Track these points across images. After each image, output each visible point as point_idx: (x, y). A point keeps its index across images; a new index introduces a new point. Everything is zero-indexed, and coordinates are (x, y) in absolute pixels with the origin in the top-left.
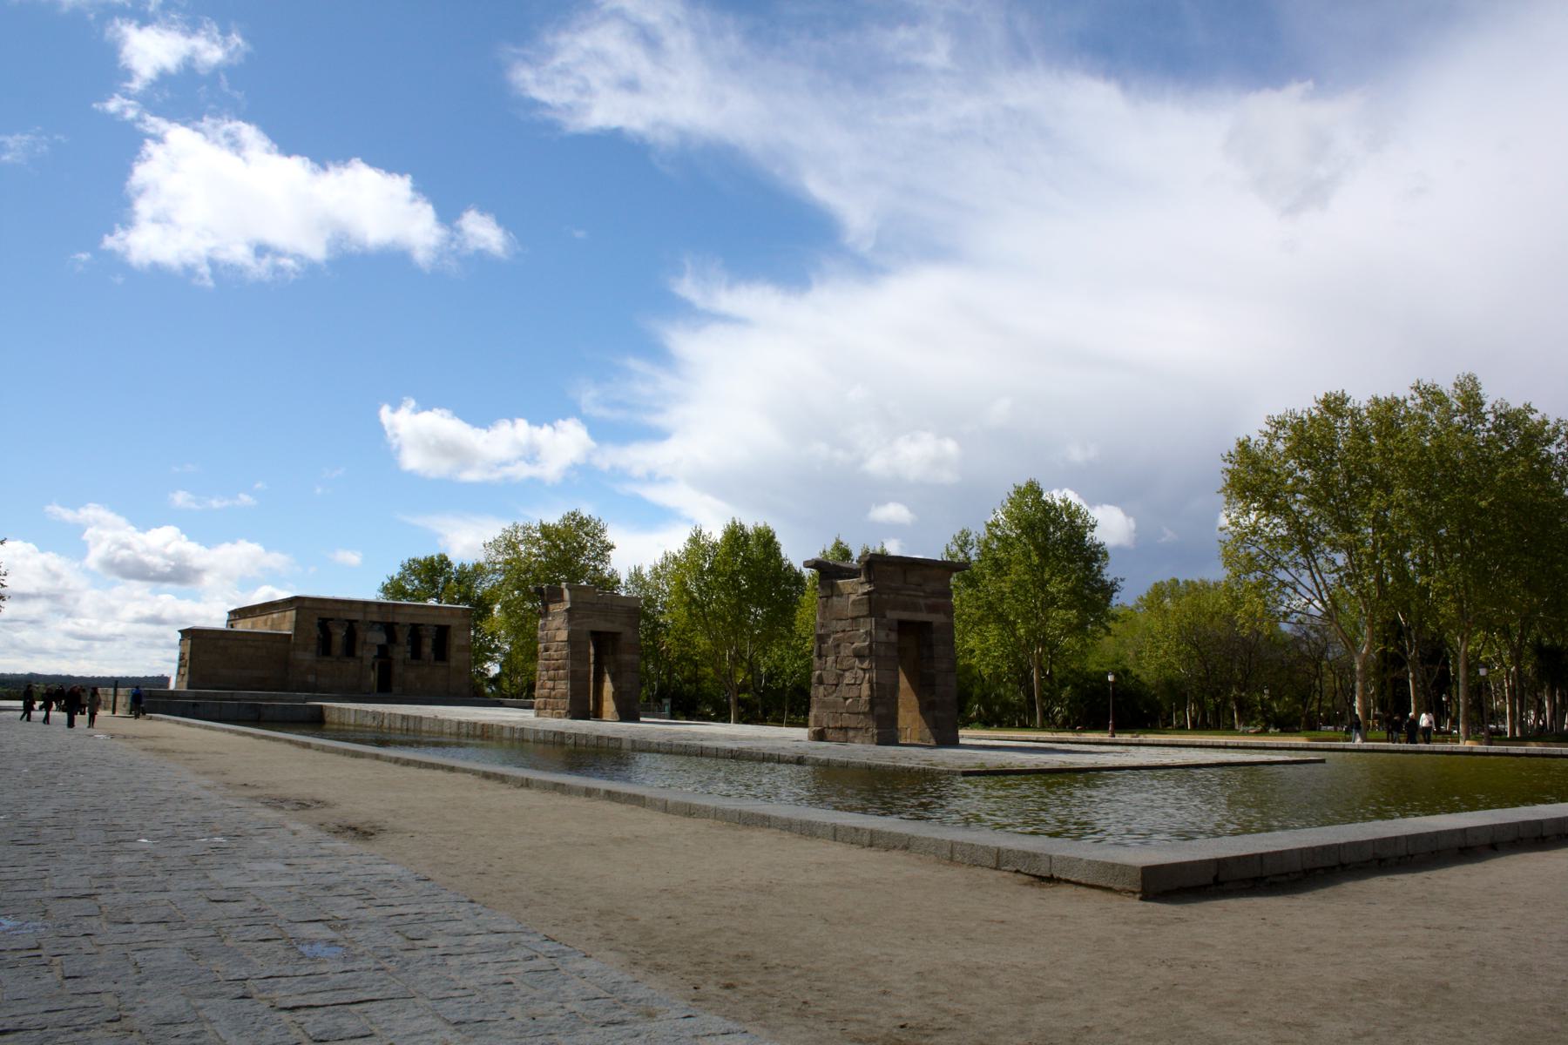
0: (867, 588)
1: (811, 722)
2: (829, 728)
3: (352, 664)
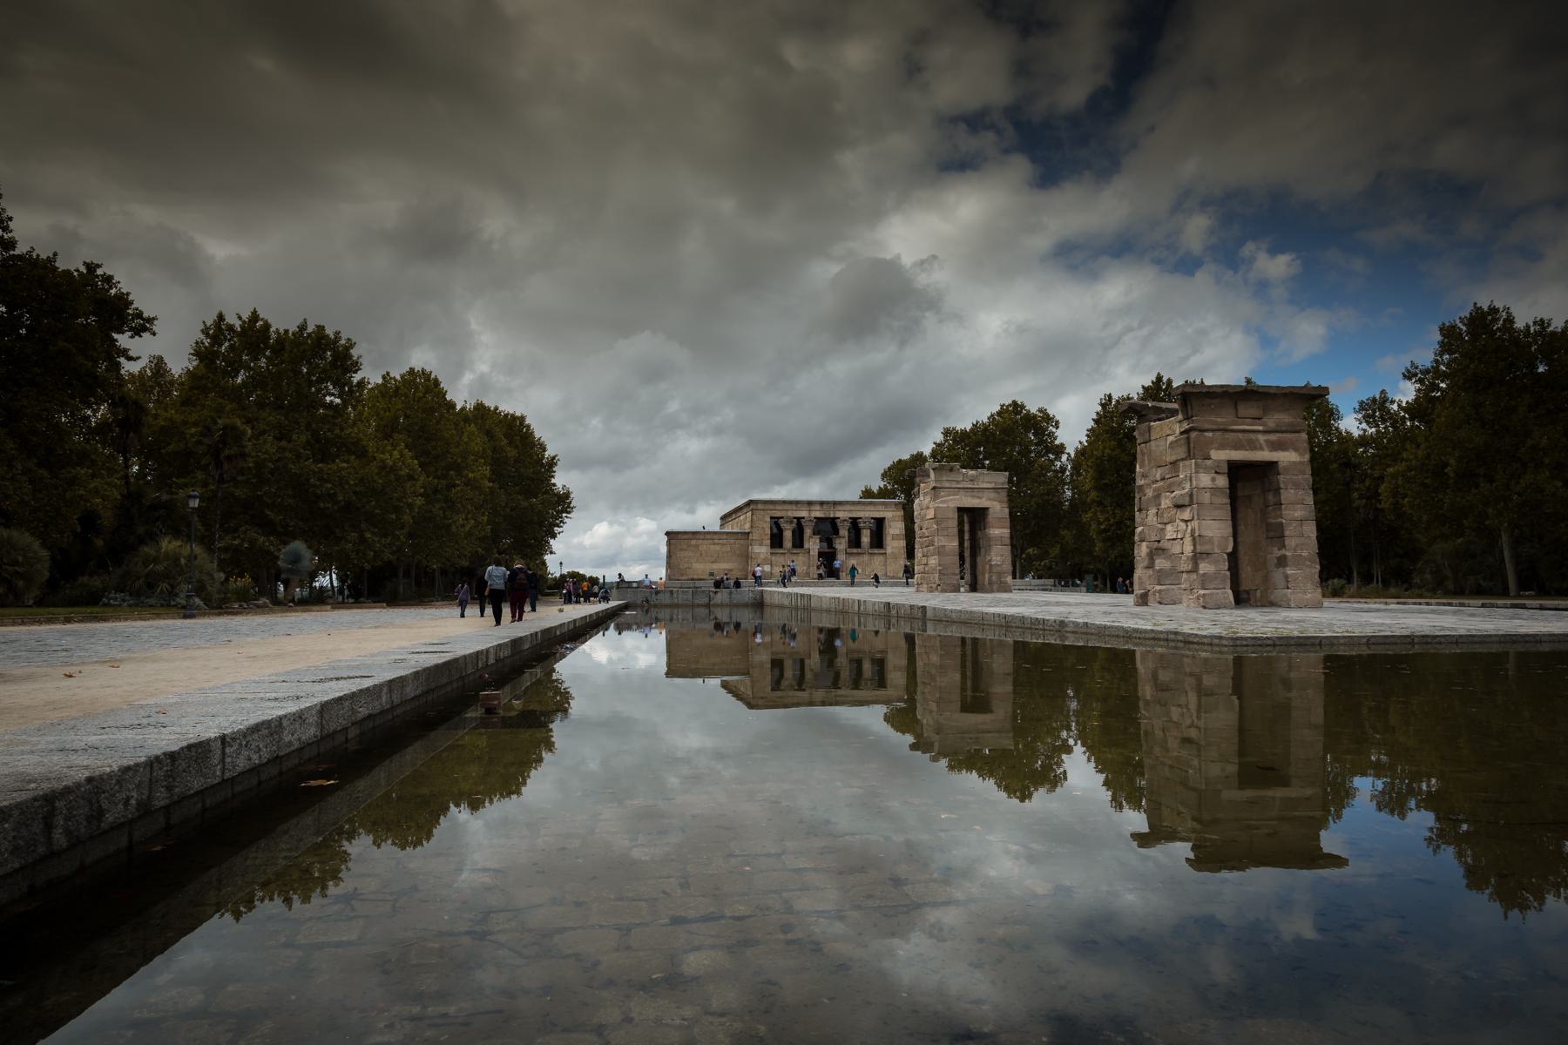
0: (1186, 426)
1: (1136, 586)
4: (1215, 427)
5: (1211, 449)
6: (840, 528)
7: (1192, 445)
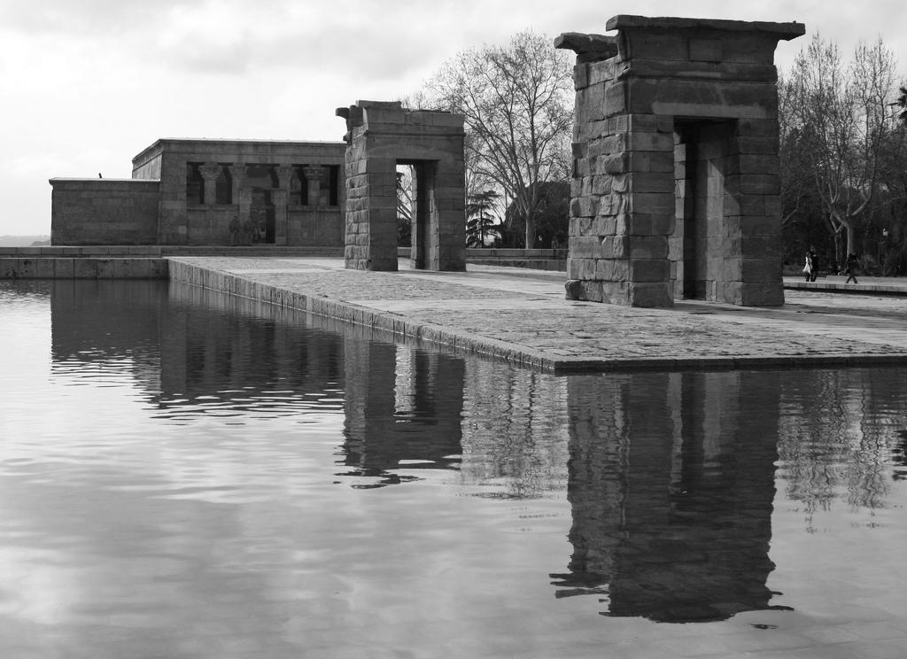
2: (585, 281)
3: (227, 213)
4: (660, 73)
5: (654, 101)
6: (280, 178)
7: (630, 95)
